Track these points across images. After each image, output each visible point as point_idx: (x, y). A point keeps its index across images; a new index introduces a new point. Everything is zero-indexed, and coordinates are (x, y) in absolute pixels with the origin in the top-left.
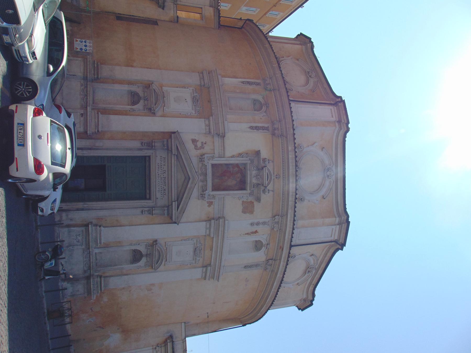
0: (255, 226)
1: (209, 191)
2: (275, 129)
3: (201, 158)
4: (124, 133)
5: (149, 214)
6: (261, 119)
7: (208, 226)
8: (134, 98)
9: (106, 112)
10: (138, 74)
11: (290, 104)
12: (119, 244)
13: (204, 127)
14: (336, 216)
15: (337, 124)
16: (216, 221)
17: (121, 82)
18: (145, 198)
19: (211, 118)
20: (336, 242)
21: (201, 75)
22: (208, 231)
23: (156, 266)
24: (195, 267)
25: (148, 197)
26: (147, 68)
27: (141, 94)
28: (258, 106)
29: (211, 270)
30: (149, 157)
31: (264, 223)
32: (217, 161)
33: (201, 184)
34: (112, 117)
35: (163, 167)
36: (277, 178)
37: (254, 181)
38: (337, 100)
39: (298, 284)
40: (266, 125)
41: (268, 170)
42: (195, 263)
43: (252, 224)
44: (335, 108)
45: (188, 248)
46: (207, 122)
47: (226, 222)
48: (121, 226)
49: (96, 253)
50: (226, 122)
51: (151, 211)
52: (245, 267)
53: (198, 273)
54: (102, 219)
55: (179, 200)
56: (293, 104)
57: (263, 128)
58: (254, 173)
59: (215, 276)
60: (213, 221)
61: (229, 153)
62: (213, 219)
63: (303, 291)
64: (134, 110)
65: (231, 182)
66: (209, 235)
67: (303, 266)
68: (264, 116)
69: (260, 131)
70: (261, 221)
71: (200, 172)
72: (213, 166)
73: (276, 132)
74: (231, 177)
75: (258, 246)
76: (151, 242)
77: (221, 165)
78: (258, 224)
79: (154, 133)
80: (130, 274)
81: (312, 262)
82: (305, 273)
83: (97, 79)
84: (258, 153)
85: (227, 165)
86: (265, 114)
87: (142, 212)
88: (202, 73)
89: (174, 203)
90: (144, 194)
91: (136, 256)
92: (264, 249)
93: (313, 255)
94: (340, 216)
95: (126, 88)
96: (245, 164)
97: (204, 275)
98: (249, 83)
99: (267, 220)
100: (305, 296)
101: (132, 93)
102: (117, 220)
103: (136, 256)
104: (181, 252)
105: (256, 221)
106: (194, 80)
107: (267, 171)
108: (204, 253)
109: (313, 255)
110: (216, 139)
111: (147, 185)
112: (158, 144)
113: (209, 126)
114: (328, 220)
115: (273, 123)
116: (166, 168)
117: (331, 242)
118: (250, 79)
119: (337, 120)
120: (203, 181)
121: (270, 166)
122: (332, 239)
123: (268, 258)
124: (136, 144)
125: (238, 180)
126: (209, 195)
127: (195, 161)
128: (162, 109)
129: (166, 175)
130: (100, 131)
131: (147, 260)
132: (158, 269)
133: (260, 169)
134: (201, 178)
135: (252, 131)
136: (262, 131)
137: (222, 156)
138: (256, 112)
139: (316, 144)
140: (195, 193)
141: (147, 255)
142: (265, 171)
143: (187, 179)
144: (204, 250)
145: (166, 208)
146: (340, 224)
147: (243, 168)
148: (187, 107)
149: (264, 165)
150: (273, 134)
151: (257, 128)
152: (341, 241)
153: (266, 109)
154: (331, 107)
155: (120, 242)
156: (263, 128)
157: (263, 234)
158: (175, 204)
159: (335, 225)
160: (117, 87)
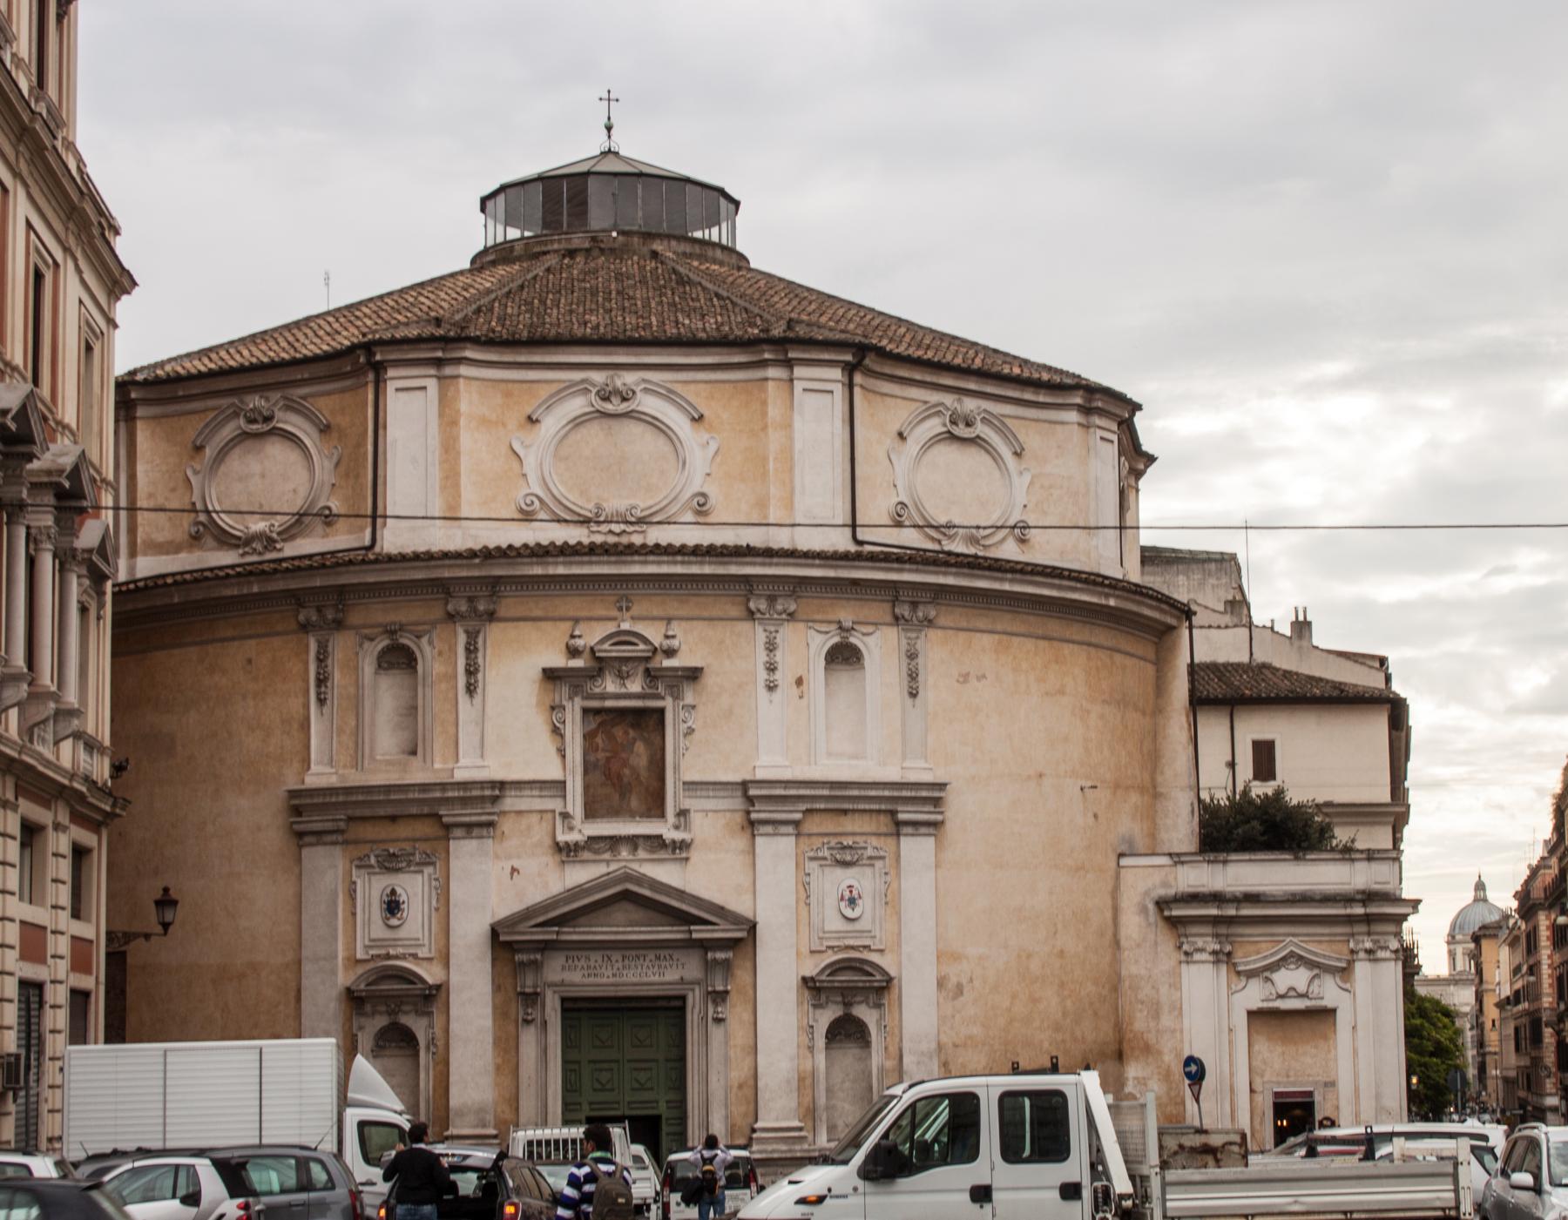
0: (778, 675)
1: (665, 829)
2: (475, 610)
3: (567, 852)
4: (498, 1068)
5: (724, 1000)
6: (440, 653)
7: (769, 829)
12: (805, 1082)
18: (683, 1009)
19: (445, 820)
20: (850, 369)
21: (307, 839)
22: (784, 829)
23: (878, 977)
25: (677, 1003)
27: (381, 1021)
28: (399, 658)
29: (908, 809)
30: (563, 1000)
31: (771, 647)
32: (575, 802)
33: (642, 854)
34: (455, 1100)
35: (592, 963)
36: (628, 609)
38: (362, 360)
39: (1018, 455)
40: (462, 639)
41: (602, 641)
42: (882, 858)
43: (771, 688)
44: (391, 373)
45: (833, 882)
46: (458, 832)
49: (829, 1141)
51: (720, 997)
53: (916, 849)
54: (733, 1126)
55: (688, 919)
57: (471, 650)
58: (610, 685)
59: (932, 795)
60: (754, 816)
61: (553, 772)
62: (748, 813)
63: (1050, 422)
64: (432, 1042)
65: (640, 755)
66: (796, 823)
67: (948, 454)
68: (430, 642)
69: (480, 661)
70: (762, 656)
71: (607, 856)
72: (591, 813)
73: (481, 608)
75: (844, 656)
76: (806, 993)
77: (586, 788)
78: (771, 668)
79: (497, 988)
80: (901, 1050)
82: (976, 441)
84: (551, 676)
85: (586, 772)
86: (424, 640)
87: (719, 1021)
88: (300, 835)
89: (695, 936)
90: (667, 1011)
91: (847, 1032)
93: (901, 435)
94: (763, 364)
96: (585, 711)
97: (923, 830)
98: (321, 681)
99: (761, 637)
100: (1073, 416)
101: (377, 1045)
102: (740, 1087)
103: (847, 1032)
105: (762, 675)
106: (327, 866)
107: (606, 646)
108: (854, 834)
109: (901, 435)
110: (510, 802)
111: (645, 1004)
112: (529, 983)
113: (469, 826)
114: (774, 412)
116: (596, 957)
117: (851, 386)
118: (307, 670)
119: (432, 371)
120: (635, 848)
121: (592, 635)
122: (838, 389)
123: (889, 618)
125: (632, 733)
126: (677, 827)
127: (580, 874)
128: (425, 964)
129: (616, 956)
130: (493, 1132)
131: (860, 1003)
132: (893, 973)
133: (601, 665)
134: (624, 854)
135: (479, 690)
136: (480, 655)
137: (559, 786)
138: (420, 668)
139: (517, 447)
140: (665, 873)
141: (847, 1005)
142: (608, 650)
143: (626, 896)
144: (841, 834)
145: (710, 955)
146: (789, 364)
147: (599, 719)
148: (414, 887)
149: (587, 654)
150: (491, 616)
151: (472, 671)
152: (849, 358)
153: (411, 632)
154: (391, 386)
155: (801, 1080)
156: (471, 650)
157: (803, 646)
158: (700, 933)
159: (791, 380)
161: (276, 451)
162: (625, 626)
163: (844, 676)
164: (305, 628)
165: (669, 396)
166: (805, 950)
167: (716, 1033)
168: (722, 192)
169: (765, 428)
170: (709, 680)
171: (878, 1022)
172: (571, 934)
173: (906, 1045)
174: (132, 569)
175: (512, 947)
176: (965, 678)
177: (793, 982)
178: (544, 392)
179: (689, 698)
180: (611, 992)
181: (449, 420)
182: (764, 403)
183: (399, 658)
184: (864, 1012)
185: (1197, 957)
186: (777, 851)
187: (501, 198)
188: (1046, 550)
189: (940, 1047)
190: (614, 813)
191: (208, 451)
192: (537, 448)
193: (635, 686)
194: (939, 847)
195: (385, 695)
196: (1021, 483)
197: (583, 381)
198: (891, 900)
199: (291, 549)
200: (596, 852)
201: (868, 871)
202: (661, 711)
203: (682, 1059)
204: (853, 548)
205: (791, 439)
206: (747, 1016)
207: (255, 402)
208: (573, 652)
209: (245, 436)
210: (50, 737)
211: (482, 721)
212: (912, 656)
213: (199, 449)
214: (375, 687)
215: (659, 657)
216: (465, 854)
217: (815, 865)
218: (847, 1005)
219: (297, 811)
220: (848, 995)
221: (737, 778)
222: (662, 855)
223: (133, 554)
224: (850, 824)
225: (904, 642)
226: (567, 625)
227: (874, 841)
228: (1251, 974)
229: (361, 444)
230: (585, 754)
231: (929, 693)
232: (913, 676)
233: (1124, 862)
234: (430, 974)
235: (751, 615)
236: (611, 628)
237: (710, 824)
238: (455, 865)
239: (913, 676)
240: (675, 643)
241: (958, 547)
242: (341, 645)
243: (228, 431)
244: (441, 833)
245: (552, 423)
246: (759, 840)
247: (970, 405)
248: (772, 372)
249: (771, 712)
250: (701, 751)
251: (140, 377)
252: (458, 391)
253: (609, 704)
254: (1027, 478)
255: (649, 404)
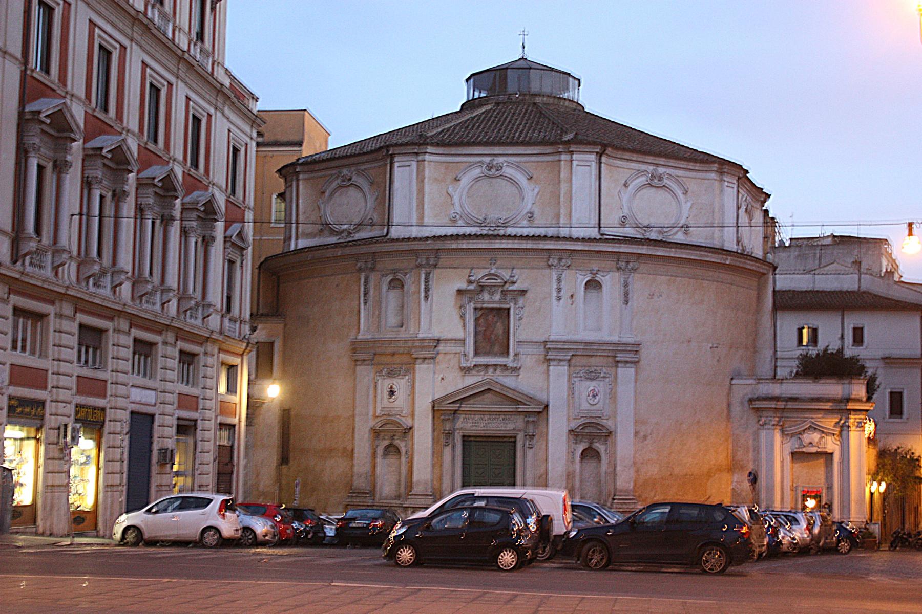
1: (509, 361)
2: (428, 264)
3: (466, 370)
4: (433, 466)
7: (555, 363)
8: (392, 450)
9: (410, 485)
10: (362, 444)
11: (393, 240)
13: (425, 366)
14: (557, 158)
15: (420, 158)
16: (551, 352)
17: (374, 467)
18: (515, 442)
20: (600, 155)
21: (359, 363)
22: (562, 363)
24: (616, 377)
25: (513, 440)
26: (353, 433)
27: (387, 443)
28: (397, 284)
29: (622, 354)
31: (559, 280)
32: (470, 349)
33: (498, 372)
34: (415, 478)
37: (497, 297)
43: (559, 299)
44: (396, 159)
45: (585, 387)
47: (552, 338)
48: (546, 474)
50: (420, 336)
52: (626, 302)
53: (625, 373)
55: (518, 402)
56: (395, 232)
58: (486, 296)
59: (635, 348)
61: (460, 335)
65: (499, 328)
72: (477, 353)
74: (492, 328)
75: (593, 285)
77: (476, 342)
78: (559, 290)
81: (642, 180)
83: (372, 493)
84: (460, 292)
88: (356, 361)
90: (509, 442)
92: (599, 278)
95: (379, 460)
96: (475, 309)
98: (365, 294)
99: (555, 277)
100: (713, 175)
104: (589, 396)
105: (555, 294)
106: (366, 374)
109: (625, 185)
110: (441, 348)
112: (448, 426)
114: (564, 175)
115: (419, 266)
121: (479, 274)
122: (594, 165)
124: (447, 451)
127: (470, 380)
132: (612, 428)
133: (482, 288)
137: (463, 341)
139: (450, 190)
140: (509, 381)
147: (480, 313)
148: (400, 384)
150: (435, 266)
151: (427, 290)
154: (396, 165)
155: (568, 476)
156: (427, 280)
157: (576, 280)
158: (522, 408)
159: (572, 161)
160: (378, 469)
161: (352, 192)
162: (493, 272)
163: (593, 294)
164: (360, 270)
165: (518, 167)
166: (571, 418)
167: (530, 453)
168: (569, 74)
169: (559, 182)
170: (528, 295)
171: (606, 450)
172: (465, 407)
173: (619, 462)
174: (296, 245)
175: (445, 412)
176: (652, 296)
177: (566, 431)
178: (463, 166)
179: (521, 302)
180: (482, 433)
181: (421, 180)
182: (559, 172)
183: (397, 284)
184: (600, 446)
185: (766, 427)
186: (559, 372)
187: (472, 80)
188: (698, 237)
189: (635, 463)
190: (487, 354)
191: (327, 194)
192: (459, 192)
193: (497, 297)
194: (637, 373)
195: (392, 299)
196: (686, 207)
197: (479, 162)
198: (613, 396)
199: (357, 236)
200: (478, 371)
201: (602, 383)
202: (509, 309)
203: (515, 463)
204: (599, 237)
205: (571, 187)
206: (544, 447)
207: (345, 171)
208: (470, 282)
209: (340, 187)
210: (200, 317)
211: (431, 311)
212: (626, 285)
213: (323, 193)
214: (387, 295)
215: (507, 285)
216: (422, 371)
217: (576, 379)
218: (591, 443)
219: (354, 351)
220: (592, 438)
221: (543, 339)
222: (507, 373)
223: (297, 239)
224: (593, 361)
225: (622, 280)
226: (467, 271)
227: (604, 370)
228: (792, 435)
229: (385, 190)
230: (475, 328)
231: (634, 302)
232: (626, 294)
233: (734, 382)
234: (409, 422)
235: (550, 266)
236: (486, 271)
237: (529, 359)
238: (417, 375)
239: (626, 294)
240: (515, 279)
241: (653, 236)
242: (373, 277)
243: (334, 185)
244: (412, 361)
245: (465, 180)
246: (551, 368)
247: (661, 170)
248: (563, 157)
249: (558, 310)
250: (525, 328)
251: (301, 161)
252: (424, 168)
253: (485, 306)
254: (689, 204)
255: (508, 171)
